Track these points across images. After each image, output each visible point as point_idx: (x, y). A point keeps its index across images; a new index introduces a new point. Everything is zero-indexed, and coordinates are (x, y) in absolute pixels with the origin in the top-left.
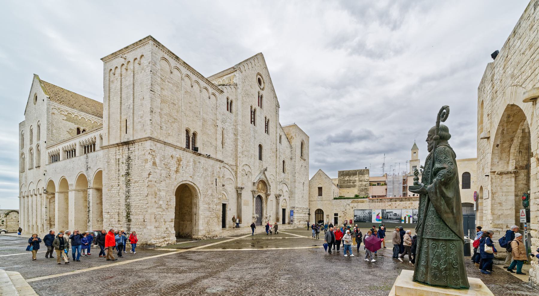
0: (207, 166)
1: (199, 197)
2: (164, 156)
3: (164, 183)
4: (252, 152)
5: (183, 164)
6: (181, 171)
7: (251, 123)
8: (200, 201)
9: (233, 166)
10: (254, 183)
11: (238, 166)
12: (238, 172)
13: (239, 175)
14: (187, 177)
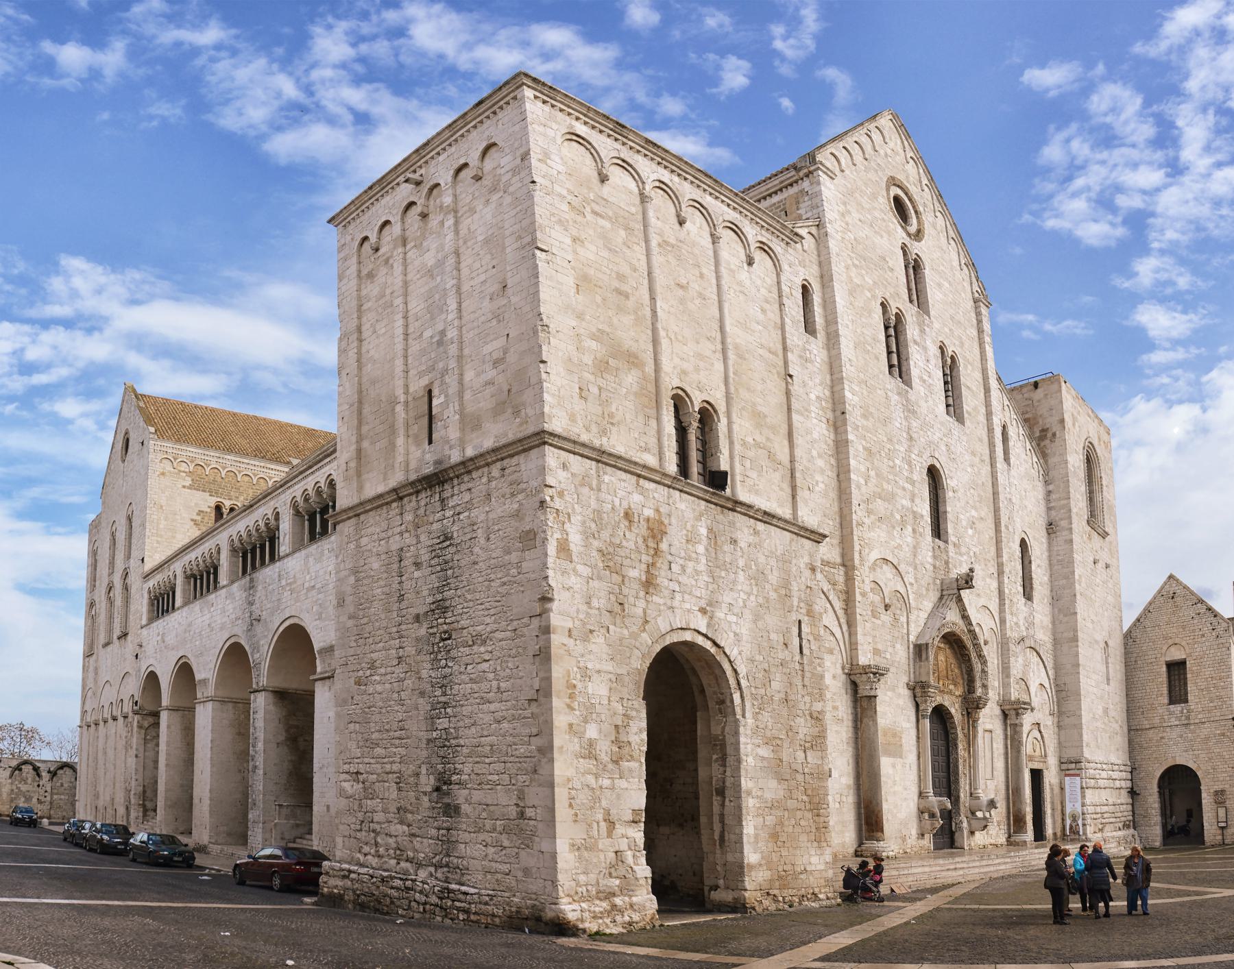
0: (762, 559)
1: (738, 710)
2: (598, 516)
3: (601, 640)
4: (904, 502)
5: (673, 551)
6: (666, 582)
7: (890, 373)
8: (742, 730)
9: (834, 566)
10: (920, 651)
11: (854, 568)
12: (858, 597)
13: (861, 609)
14: (689, 611)
